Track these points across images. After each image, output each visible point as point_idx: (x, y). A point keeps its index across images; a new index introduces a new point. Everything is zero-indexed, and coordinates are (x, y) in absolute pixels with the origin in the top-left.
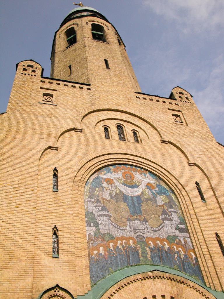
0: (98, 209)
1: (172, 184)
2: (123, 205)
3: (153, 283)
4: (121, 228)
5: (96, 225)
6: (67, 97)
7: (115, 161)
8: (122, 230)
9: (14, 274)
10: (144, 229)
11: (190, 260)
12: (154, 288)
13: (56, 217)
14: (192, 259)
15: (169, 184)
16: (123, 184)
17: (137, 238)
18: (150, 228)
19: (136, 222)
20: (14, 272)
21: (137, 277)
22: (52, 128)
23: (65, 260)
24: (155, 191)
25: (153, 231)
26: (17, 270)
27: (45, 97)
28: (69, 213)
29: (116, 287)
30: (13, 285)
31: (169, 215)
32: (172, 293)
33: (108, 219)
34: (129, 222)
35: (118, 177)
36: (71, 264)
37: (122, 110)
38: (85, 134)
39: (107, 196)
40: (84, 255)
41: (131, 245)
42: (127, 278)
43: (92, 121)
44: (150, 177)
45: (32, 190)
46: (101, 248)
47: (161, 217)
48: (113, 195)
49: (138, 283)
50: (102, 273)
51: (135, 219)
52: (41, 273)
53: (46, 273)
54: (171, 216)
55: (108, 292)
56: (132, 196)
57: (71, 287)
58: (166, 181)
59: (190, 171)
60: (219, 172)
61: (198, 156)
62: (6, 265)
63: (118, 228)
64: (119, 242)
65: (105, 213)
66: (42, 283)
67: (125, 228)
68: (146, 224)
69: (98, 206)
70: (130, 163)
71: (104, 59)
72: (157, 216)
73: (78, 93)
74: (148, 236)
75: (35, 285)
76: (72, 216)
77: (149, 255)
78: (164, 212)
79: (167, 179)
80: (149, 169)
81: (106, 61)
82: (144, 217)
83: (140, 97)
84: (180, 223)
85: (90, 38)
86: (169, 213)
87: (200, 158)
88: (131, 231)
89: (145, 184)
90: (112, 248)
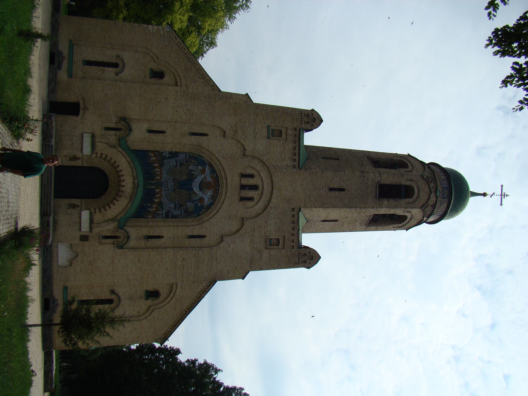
0: (181, 161)
1: (203, 216)
2: (185, 177)
4: (168, 173)
5: (170, 158)
6: (280, 148)
7: (220, 178)
8: (167, 174)
10: (167, 188)
13: (172, 133)
15: (204, 215)
16: (202, 181)
17: (162, 182)
18: (168, 192)
19: (173, 184)
22: (243, 135)
24: (198, 203)
25: (166, 194)
27: (279, 131)
28: (175, 141)
29: (130, 160)
31: (179, 208)
33: (174, 166)
34: (172, 179)
35: (208, 178)
37: (274, 191)
38: (242, 158)
39: (191, 167)
41: (157, 177)
43: (257, 166)
44: (210, 202)
45: (189, 120)
46: (154, 159)
47: (177, 202)
48: (192, 172)
51: (174, 183)
54: (178, 210)
55: (127, 156)
56: (193, 185)
58: (206, 213)
59: (216, 235)
60: (216, 259)
61: (231, 246)
63: (168, 170)
64: (159, 170)
65: (178, 164)
66: (133, 124)
67: (168, 175)
68: (171, 190)
69: (183, 161)
70: (220, 189)
71: (344, 187)
72: (178, 199)
73: (287, 157)
74: (163, 190)
76: (173, 142)
77: (149, 187)
78: (180, 206)
79: (207, 214)
80: (216, 202)
81: (343, 190)
82: (177, 190)
83: (294, 212)
84: (172, 215)
85: (379, 179)
86: (180, 209)
87: (229, 247)
88: (166, 179)
89: (203, 197)
90: (155, 165)
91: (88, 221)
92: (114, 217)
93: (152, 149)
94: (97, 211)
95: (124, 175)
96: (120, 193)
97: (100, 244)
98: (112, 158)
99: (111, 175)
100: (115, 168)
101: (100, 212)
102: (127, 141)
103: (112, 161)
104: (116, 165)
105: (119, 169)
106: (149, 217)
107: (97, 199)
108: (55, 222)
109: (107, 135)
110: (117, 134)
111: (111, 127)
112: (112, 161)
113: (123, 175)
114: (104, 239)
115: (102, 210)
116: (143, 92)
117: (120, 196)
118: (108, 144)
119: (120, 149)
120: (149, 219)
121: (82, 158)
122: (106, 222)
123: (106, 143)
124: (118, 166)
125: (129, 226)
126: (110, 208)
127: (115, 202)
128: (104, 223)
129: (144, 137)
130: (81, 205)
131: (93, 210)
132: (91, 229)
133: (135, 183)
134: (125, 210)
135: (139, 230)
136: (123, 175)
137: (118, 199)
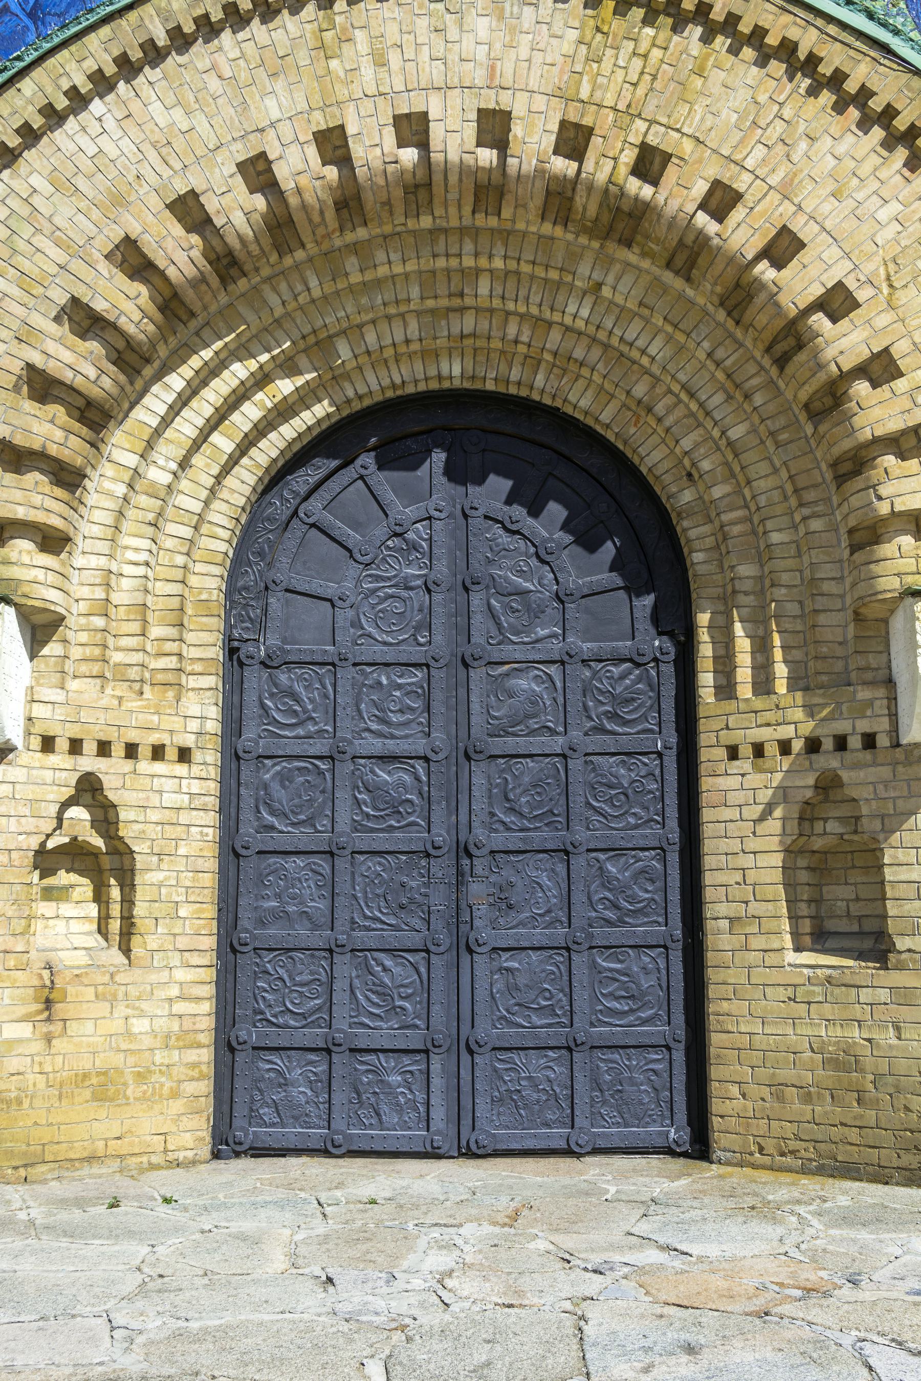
32: (584, 94)
95: (320, 122)
98: (62, 298)
137: (700, 188)
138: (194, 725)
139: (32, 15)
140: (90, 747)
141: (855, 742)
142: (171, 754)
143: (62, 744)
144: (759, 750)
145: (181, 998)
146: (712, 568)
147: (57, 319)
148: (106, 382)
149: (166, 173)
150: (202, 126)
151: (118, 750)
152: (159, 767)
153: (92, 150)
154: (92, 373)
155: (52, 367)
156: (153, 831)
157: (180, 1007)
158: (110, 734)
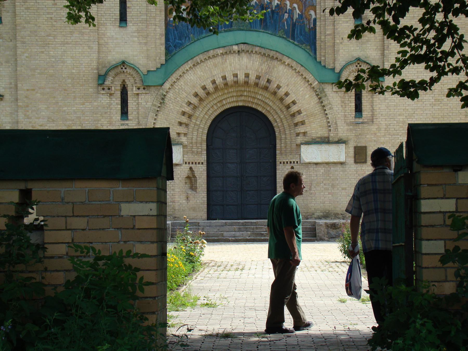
3: (237, 59)
9: (77, 50)
11: (306, 22)
12: (237, 65)
14: (309, 20)
20: (77, 48)
21: (217, 52)
23: (134, 29)
26: (79, 45)
29: (190, 64)
30: (77, 62)
36: (141, 34)
40: (158, 20)
42: (205, 53)
49: (219, 60)
50: (180, 42)
52: (107, 46)
53: (112, 46)
55: (180, 70)
57: (141, 62)
62: (67, 40)
66: (109, 58)
75: (100, 60)
91: (325, 147)
92: (315, 94)
93: (163, 13)
94: (301, 129)
95: (222, 75)
96: (263, 82)
97: (373, 122)
98: (186, 101)
99: (224, 102)
100: (208, 94)
101: (303, 123)
102: (148, 71)
103: (194, 101)
104: (202, 93)
105: (210, 87)
106: (314, 17)
107: (276, 130)
108: (326, 216)
109: (138, 113)
110: (135, 92)
111: (120, 106)
112: (194, 101)
113: (222, 77)
114: (363, 113)
115: (298, 119)
116: (37, 38)
117: (269, 81)
118: (158, 111)
119: (167, 85)
120: (318, 16)
121: (191, 165)
122: (325, 110)
123: (156, 115)
124: (204, 88)
125: (335, 60)
126: (294, 103)
127: (281, 92)
128: (327, 114)
129: (136, 34)
130: (291, 162)
131: (300, 139)
132: (340, 142)
133: (239, 51)
134: (298, 69)
135: (342, 39)
136: (224, 78)
137: (276, 85)
138: (203, 159)
139: (174, 47)
140: (191, 163)
141: (295, 162)
142: (201, 163)
143: (188, 163)
144: (284, 163)
145: (203, 198)
146: (279, 135)
147: (186, 104)
148: (193, 112)
149: (201, 82)
150: (205, 75)
151: (194, 163)
152: (199, 165)
153: (190, 78)
154: (191, 112)
155: (186, 111)
156: (199, 174)
157: (203, 199)
158: (193, 161)
